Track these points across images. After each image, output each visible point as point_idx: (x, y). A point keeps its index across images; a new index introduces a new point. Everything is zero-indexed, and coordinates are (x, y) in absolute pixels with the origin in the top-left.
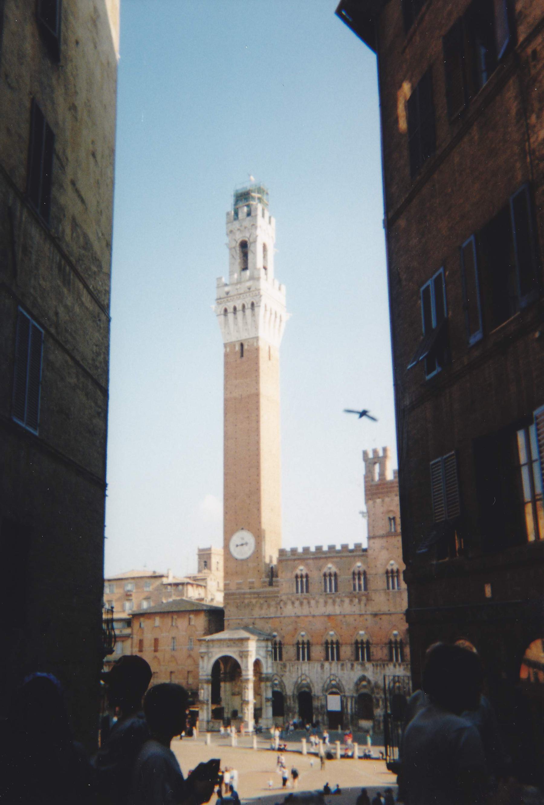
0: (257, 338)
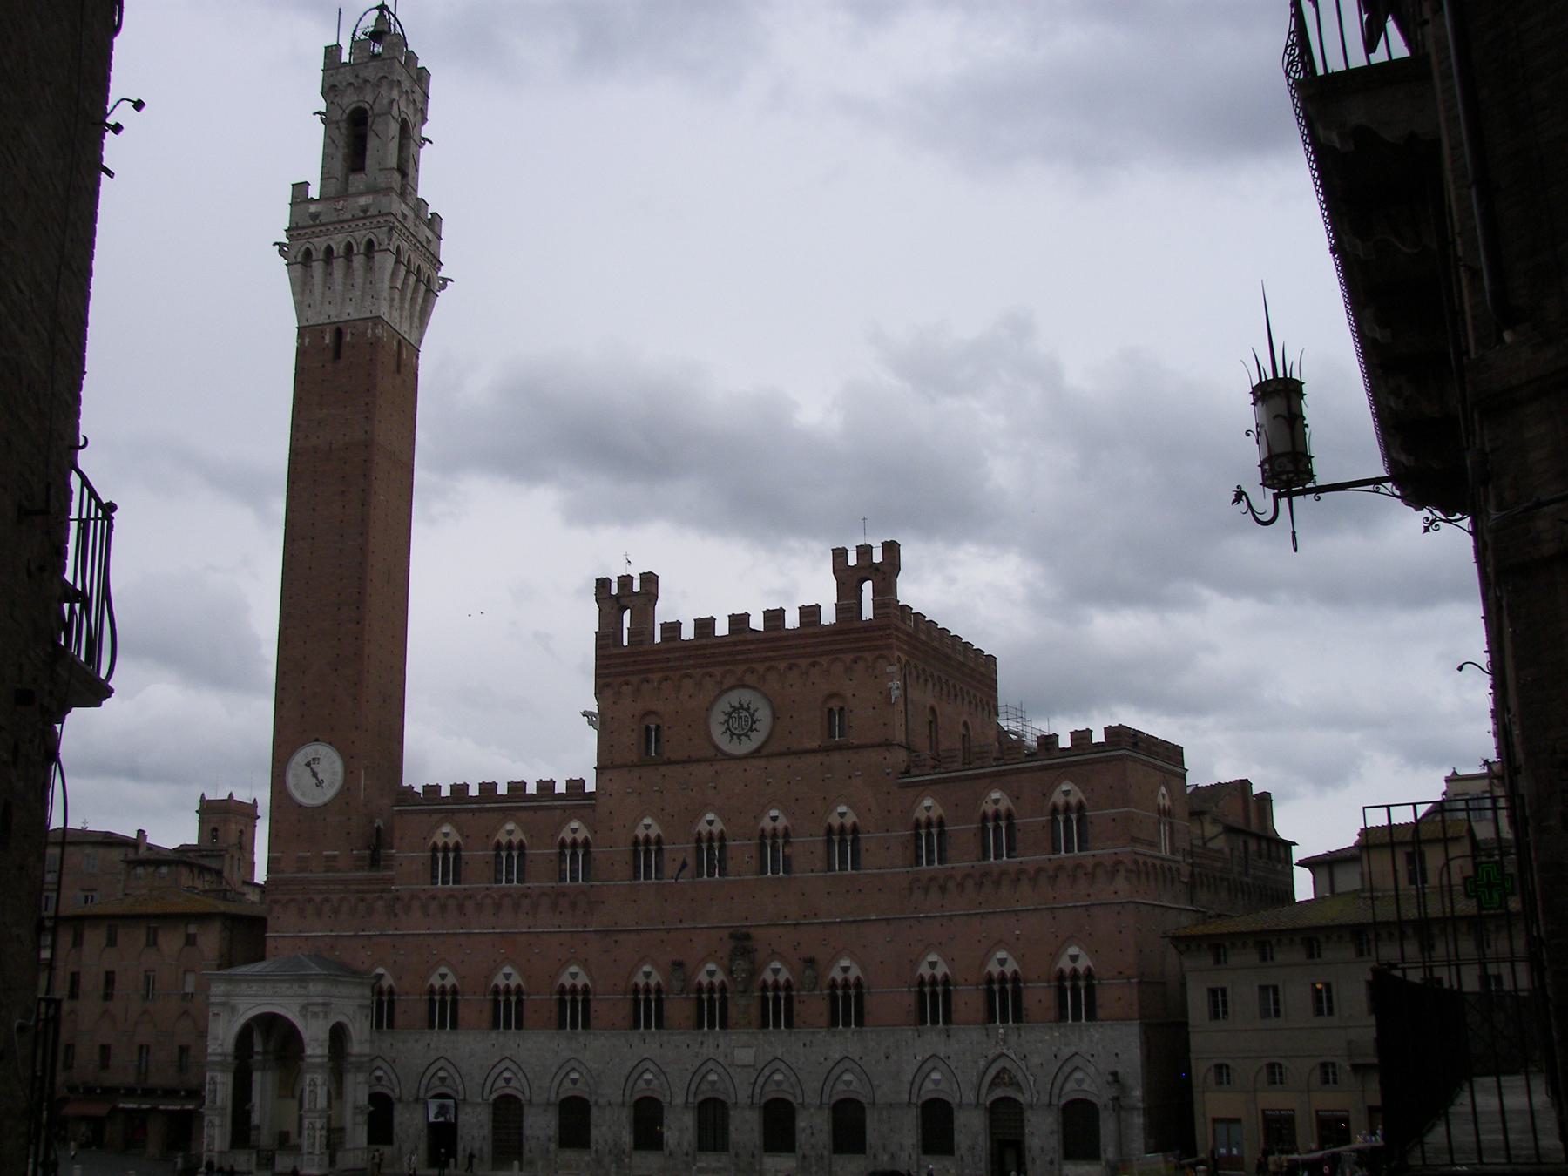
0: (377, 320)
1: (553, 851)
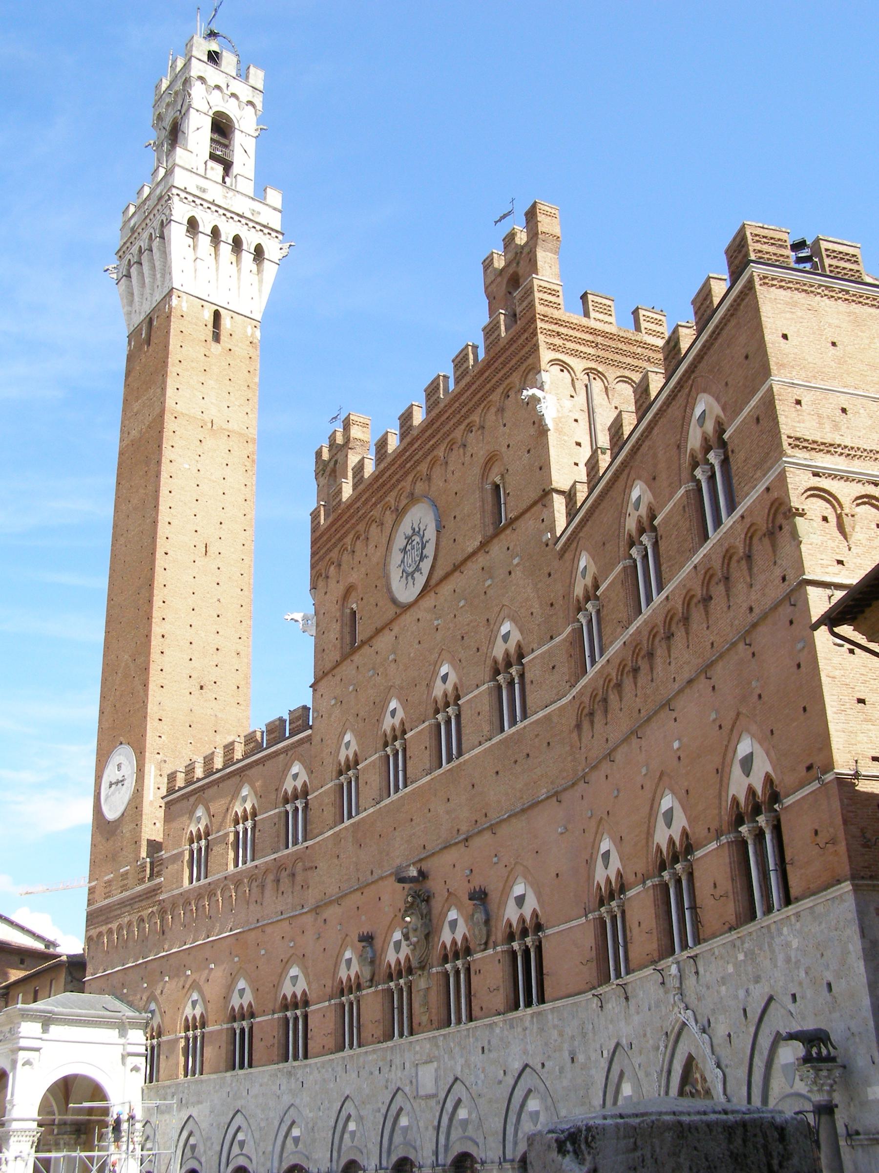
1: (277, 810)
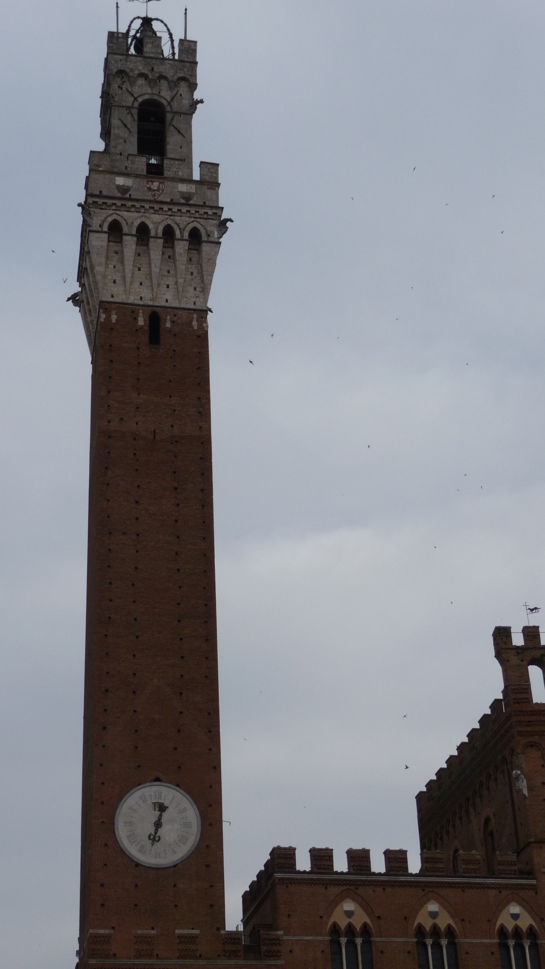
0: (203, 312)
